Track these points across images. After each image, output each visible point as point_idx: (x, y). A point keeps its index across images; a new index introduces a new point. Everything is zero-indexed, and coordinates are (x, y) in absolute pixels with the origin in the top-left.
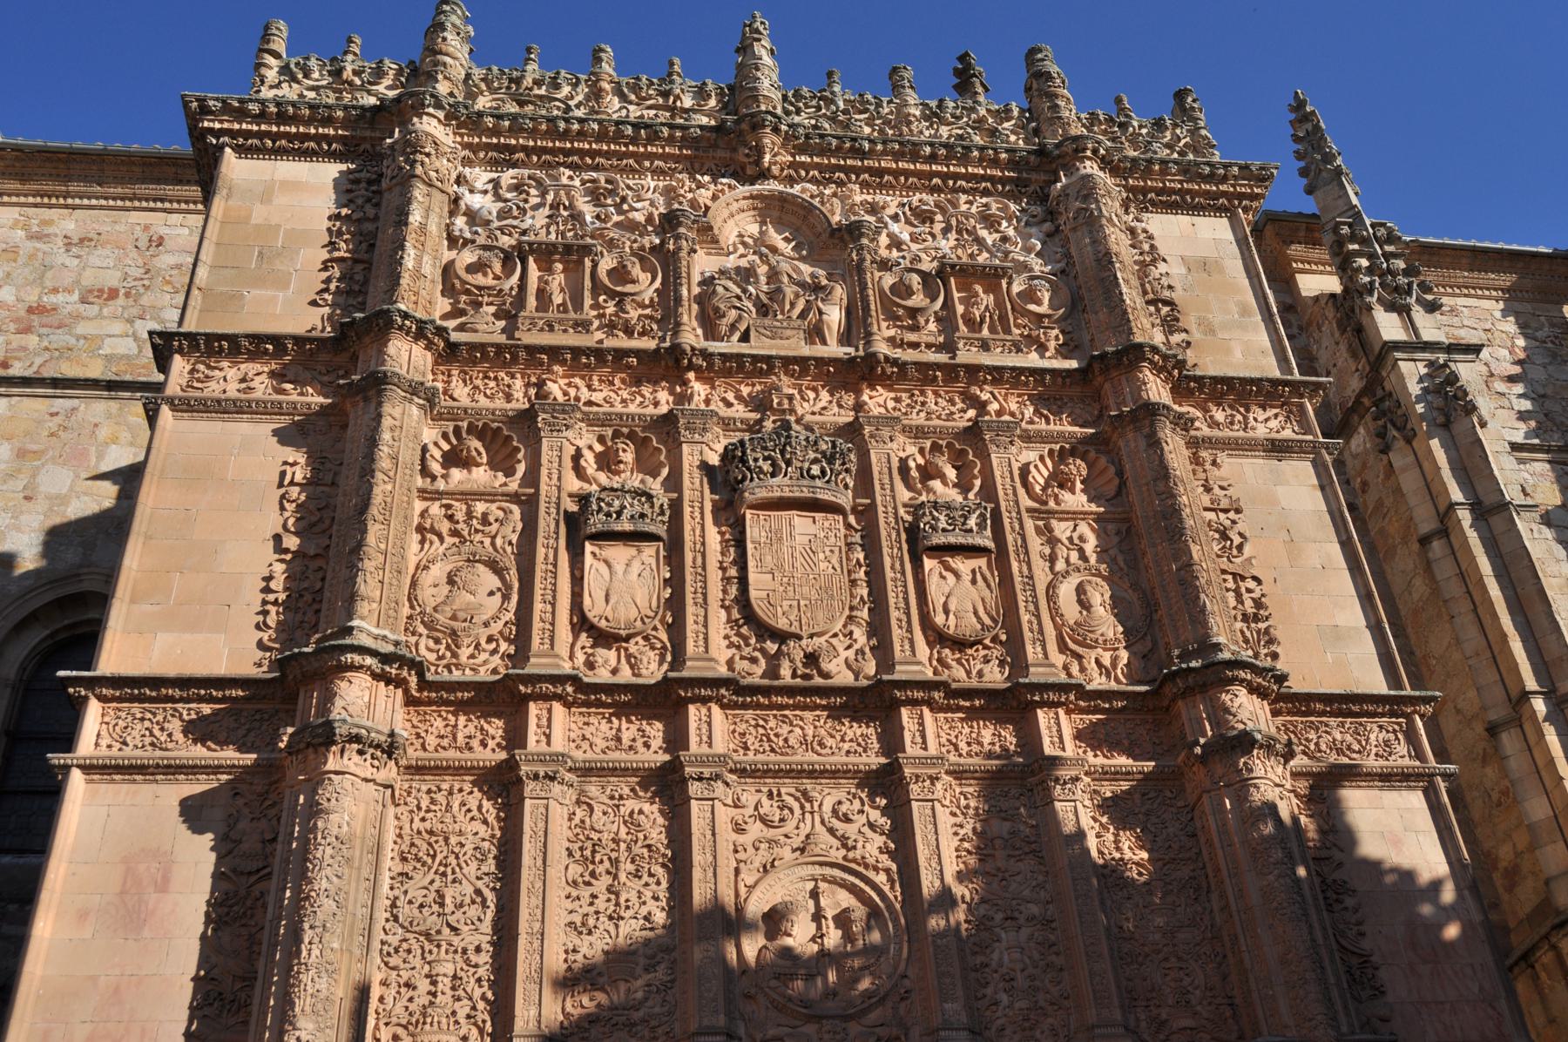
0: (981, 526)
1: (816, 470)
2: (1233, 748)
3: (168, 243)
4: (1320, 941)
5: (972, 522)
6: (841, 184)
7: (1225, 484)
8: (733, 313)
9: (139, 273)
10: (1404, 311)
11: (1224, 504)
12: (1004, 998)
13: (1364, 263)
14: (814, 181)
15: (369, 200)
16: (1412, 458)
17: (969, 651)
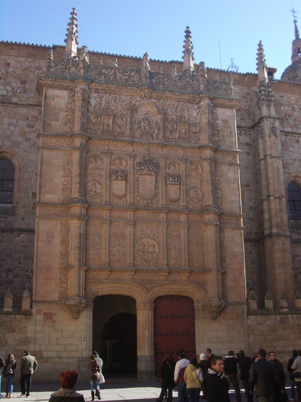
0: (178, 180)
1: (151, 169)
2: (211, 225)
3: (11, 65)
4: (218, 255)
5: (176, 180)
6: (160, 99)
7: (220, 171)
8: (139, 131)
9: (4, 72)
10: (269, 106)
11: (219, 175)
12: (172, 260)
13: (263, 92)
14: (155, 99)
15: (72, 101)
16: (262, 142)
17: (173, 203)
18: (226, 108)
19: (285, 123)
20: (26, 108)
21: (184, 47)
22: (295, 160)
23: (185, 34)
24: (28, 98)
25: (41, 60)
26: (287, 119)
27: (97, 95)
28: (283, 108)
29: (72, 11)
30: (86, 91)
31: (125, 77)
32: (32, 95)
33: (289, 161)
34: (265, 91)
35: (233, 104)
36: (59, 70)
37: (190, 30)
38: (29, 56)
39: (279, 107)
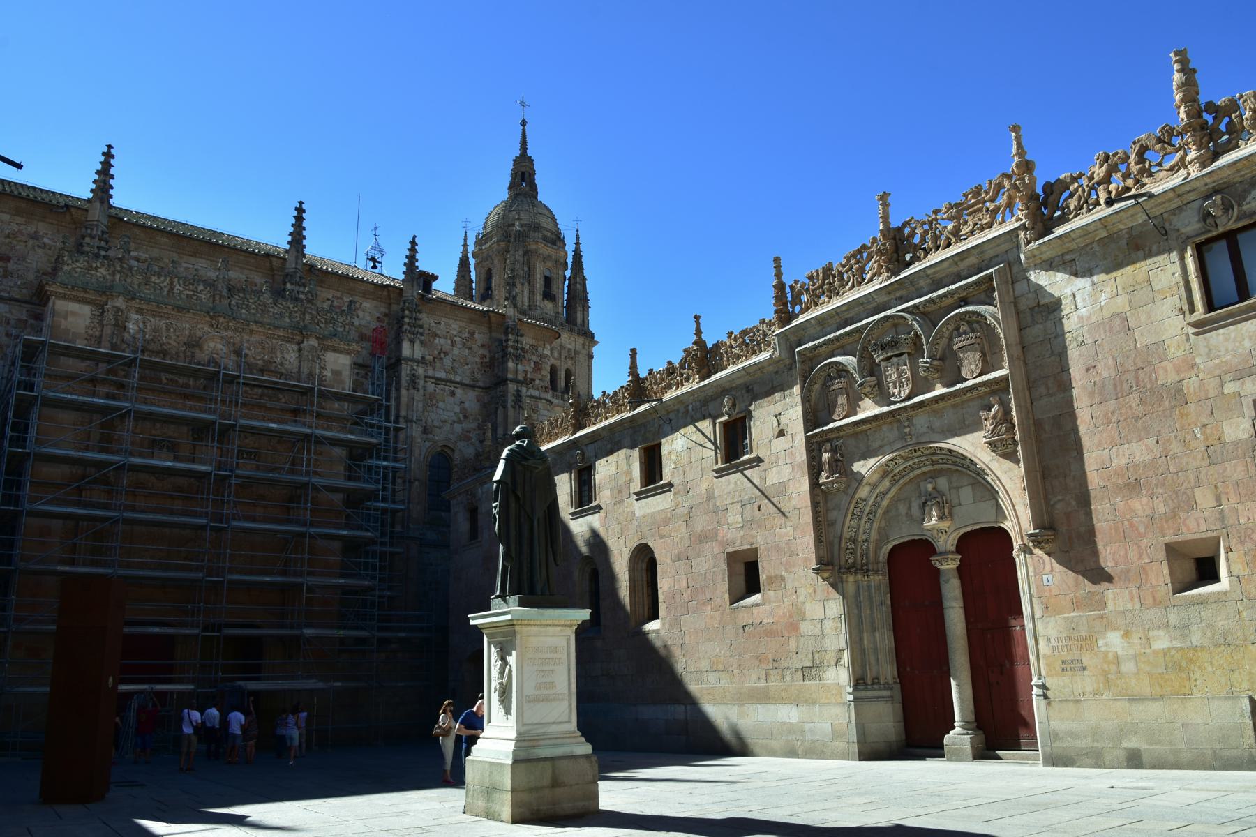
10: (412, 342)
18: (341, 352)
19: (438, 365)
20: (7, 303)
21: (291, 234)
22: (445, 421)
23: (295, 213)
24: (11, 287)
25: (40, 223)
26: (442, 359)
27: (139, 317)
28: (437, 341)
29: (105, 150)
30: (122, 311)
31: (188, 292)
32: (19, 283)
33: (436, 424)
34: (410, 318)
35: (351, 348)
36: (78, 270)
37: (304, 207)
38: (18, 212)
39: (432, 339)
